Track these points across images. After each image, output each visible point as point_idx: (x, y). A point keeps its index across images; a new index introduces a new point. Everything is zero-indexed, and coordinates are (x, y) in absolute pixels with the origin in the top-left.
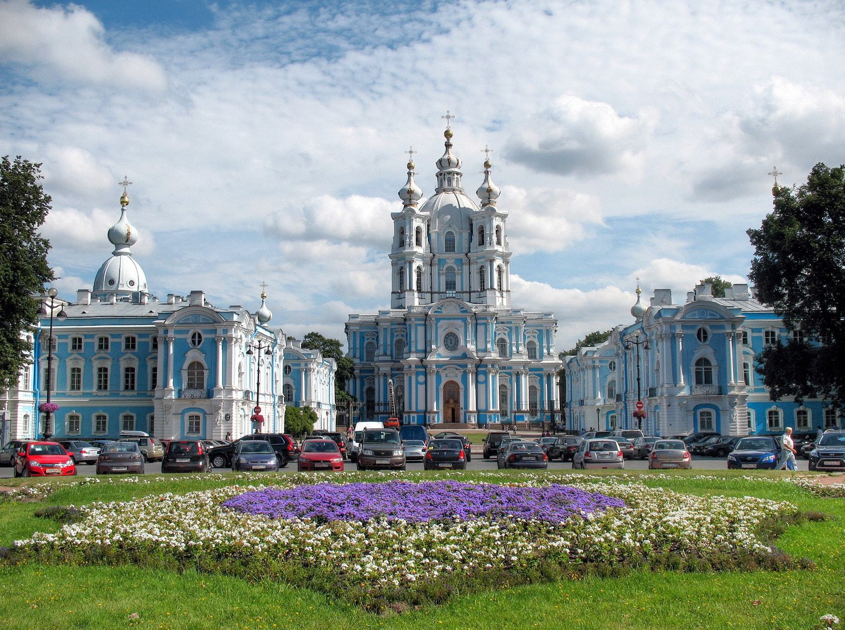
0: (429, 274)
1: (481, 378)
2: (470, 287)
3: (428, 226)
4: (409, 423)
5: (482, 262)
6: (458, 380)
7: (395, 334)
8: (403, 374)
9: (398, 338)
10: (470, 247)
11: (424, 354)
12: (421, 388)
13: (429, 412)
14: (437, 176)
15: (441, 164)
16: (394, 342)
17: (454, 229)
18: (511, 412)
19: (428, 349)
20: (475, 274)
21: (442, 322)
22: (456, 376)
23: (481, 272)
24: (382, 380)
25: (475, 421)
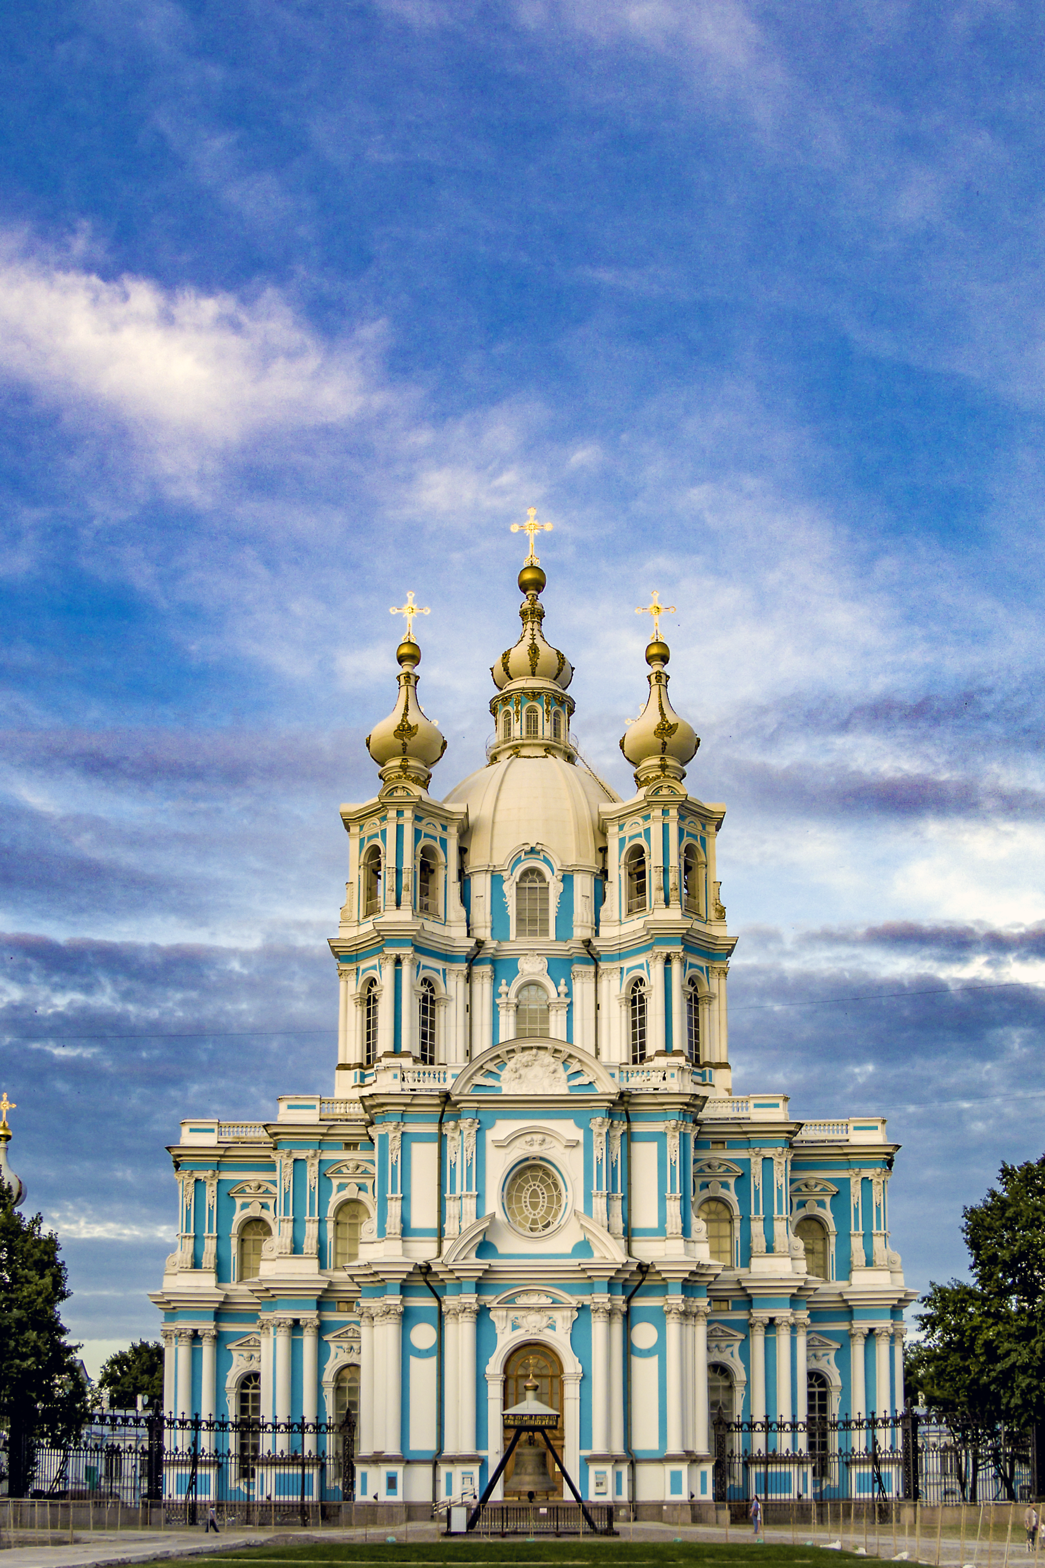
0: (461, 1008)
1: (644, 1335)
2: (597, 1052)
3: (463, 851)
4: (375, 1497)
5: (641, 966)
6: (560, 1339)
7: (335, 1182)
8: (358, 1323)
9: (346, 1194)
10: (597, 922)
11: (434, 1246)
12: (423, 1370)
13: (453, 1460)
14: (494, 711)
15: (507, 673)
16: (330, 1212)
17: (546, 861)
18: (746, 1465)
19: (451, 1227)
20: (615, 1004)
21: (502, 1129)
22: (552, 1327)
23: (634, 1002)
24: (283, 1340)
25: (619, 1491)
